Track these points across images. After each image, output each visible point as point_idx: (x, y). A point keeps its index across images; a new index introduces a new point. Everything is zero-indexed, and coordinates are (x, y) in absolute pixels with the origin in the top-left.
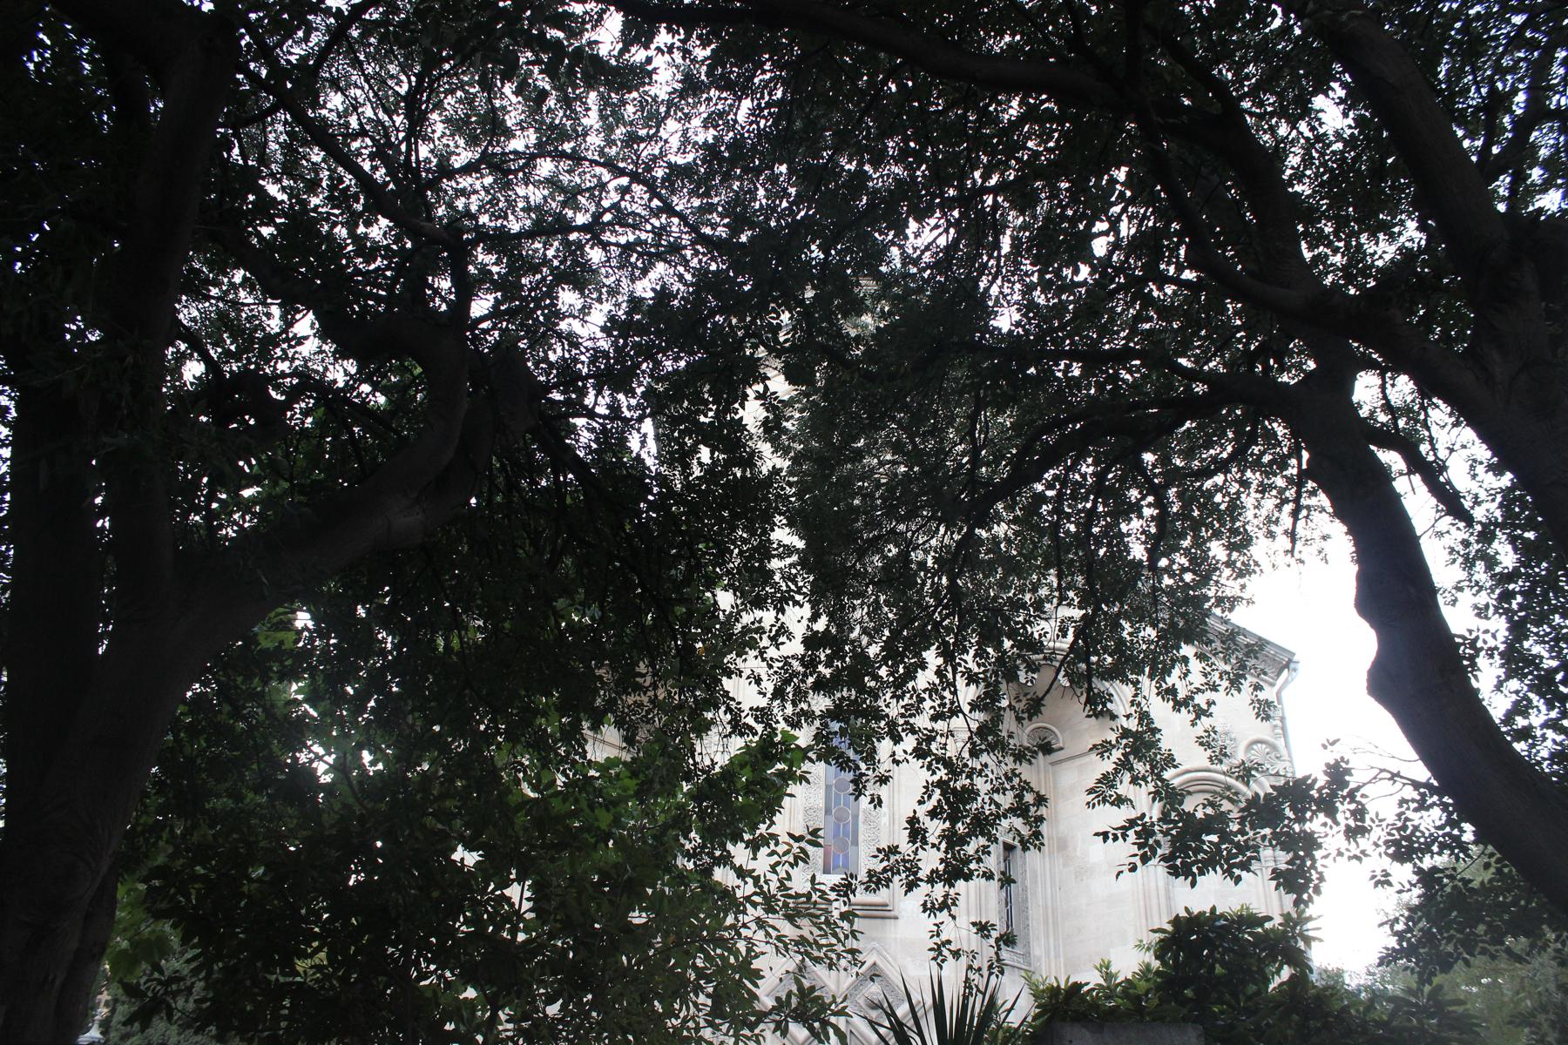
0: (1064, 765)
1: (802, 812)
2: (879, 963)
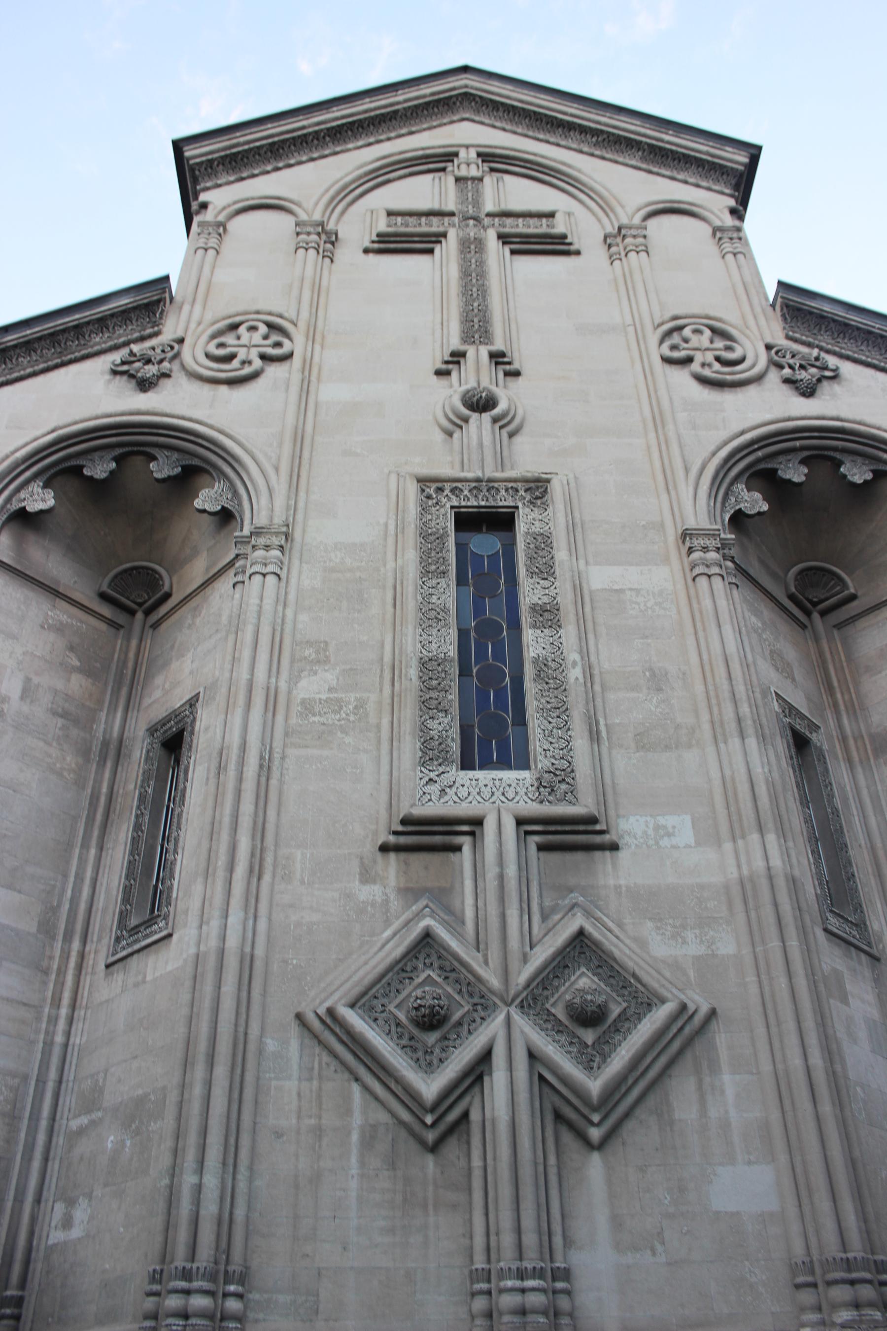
0: (862, 623)
1: (414, 663)
2: (589, 928)
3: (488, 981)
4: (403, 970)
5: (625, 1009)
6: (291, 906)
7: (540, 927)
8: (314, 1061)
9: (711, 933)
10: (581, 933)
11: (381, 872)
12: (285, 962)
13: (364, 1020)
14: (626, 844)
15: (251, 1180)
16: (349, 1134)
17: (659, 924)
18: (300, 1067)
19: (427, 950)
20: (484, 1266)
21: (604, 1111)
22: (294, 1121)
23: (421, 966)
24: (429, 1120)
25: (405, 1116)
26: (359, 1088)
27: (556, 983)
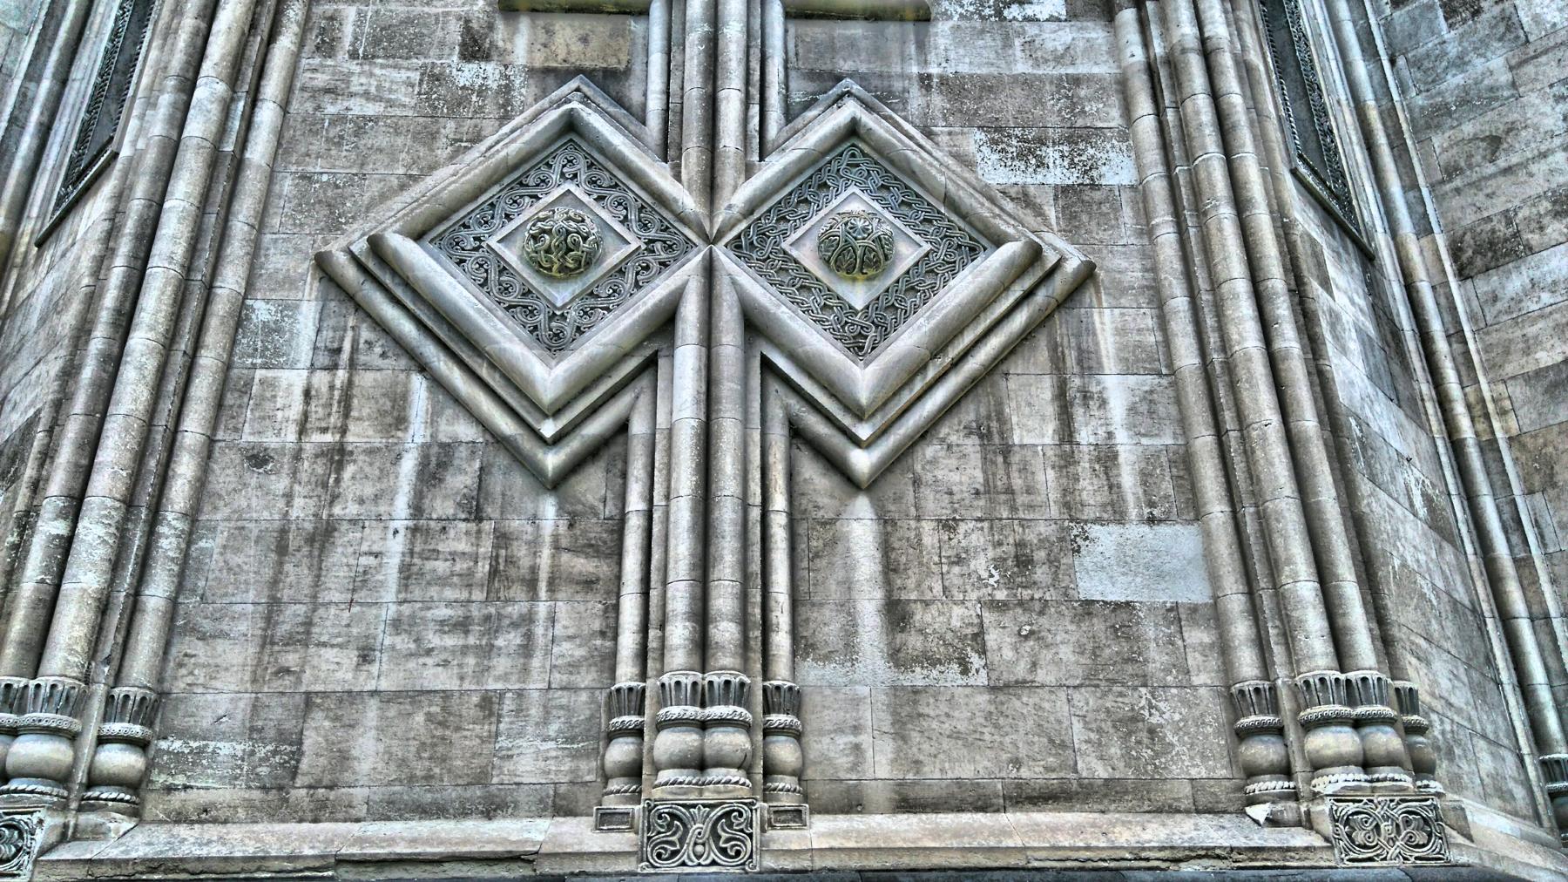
2: (868, 119)
3: (676, 201)
4: (521, 184)
5: (927, 255)
6: (327, 91)
7: (780, 130)
8: (342, 339)
9: (1091, 151)
10: (853, 130)
11: (500, 44)
12: (307, 178)
13: (437, 260)
14: (945, 13)
15: (190, 538)
16: (399, 457)
17: (996, 136)
18: (315, 348)
19: (570, 153)
20: (633, 684)
21: (879, 421)
22: (291, 436)
23: (555, 177)
24: (549, 429)
25: (506, 425)
26: (425, 384)
27: (802, 210)
